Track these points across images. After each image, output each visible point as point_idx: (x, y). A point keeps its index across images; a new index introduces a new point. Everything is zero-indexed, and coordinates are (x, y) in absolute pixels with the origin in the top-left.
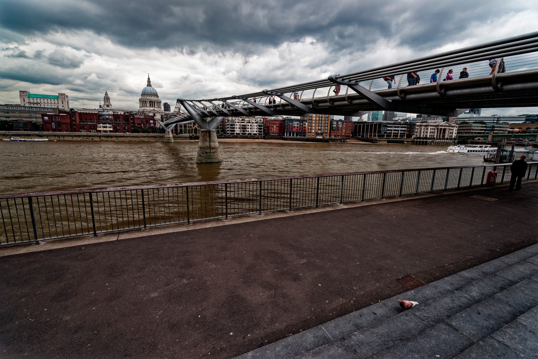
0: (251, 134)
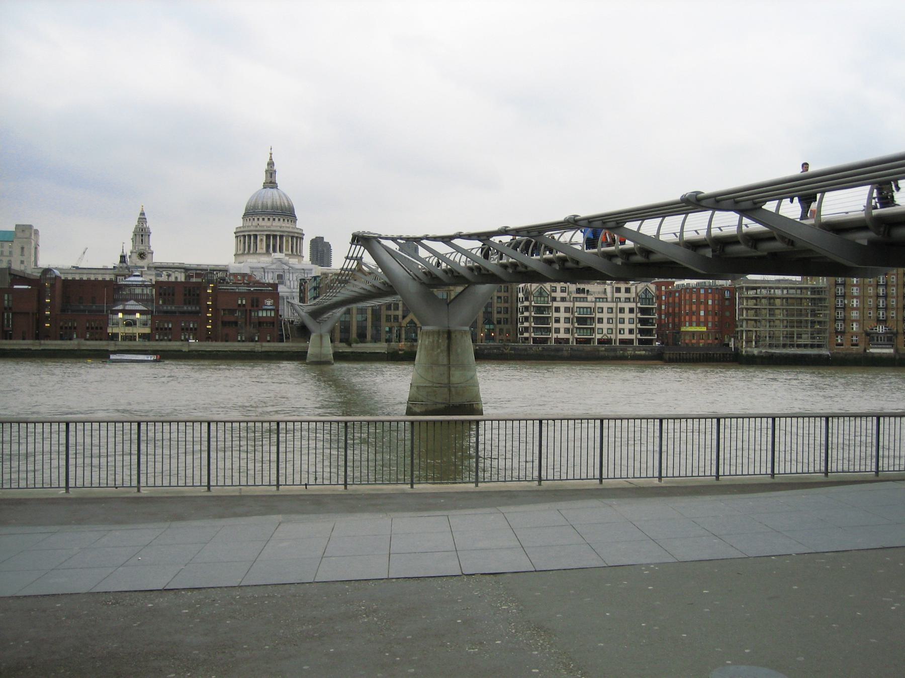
0: (609, 341)
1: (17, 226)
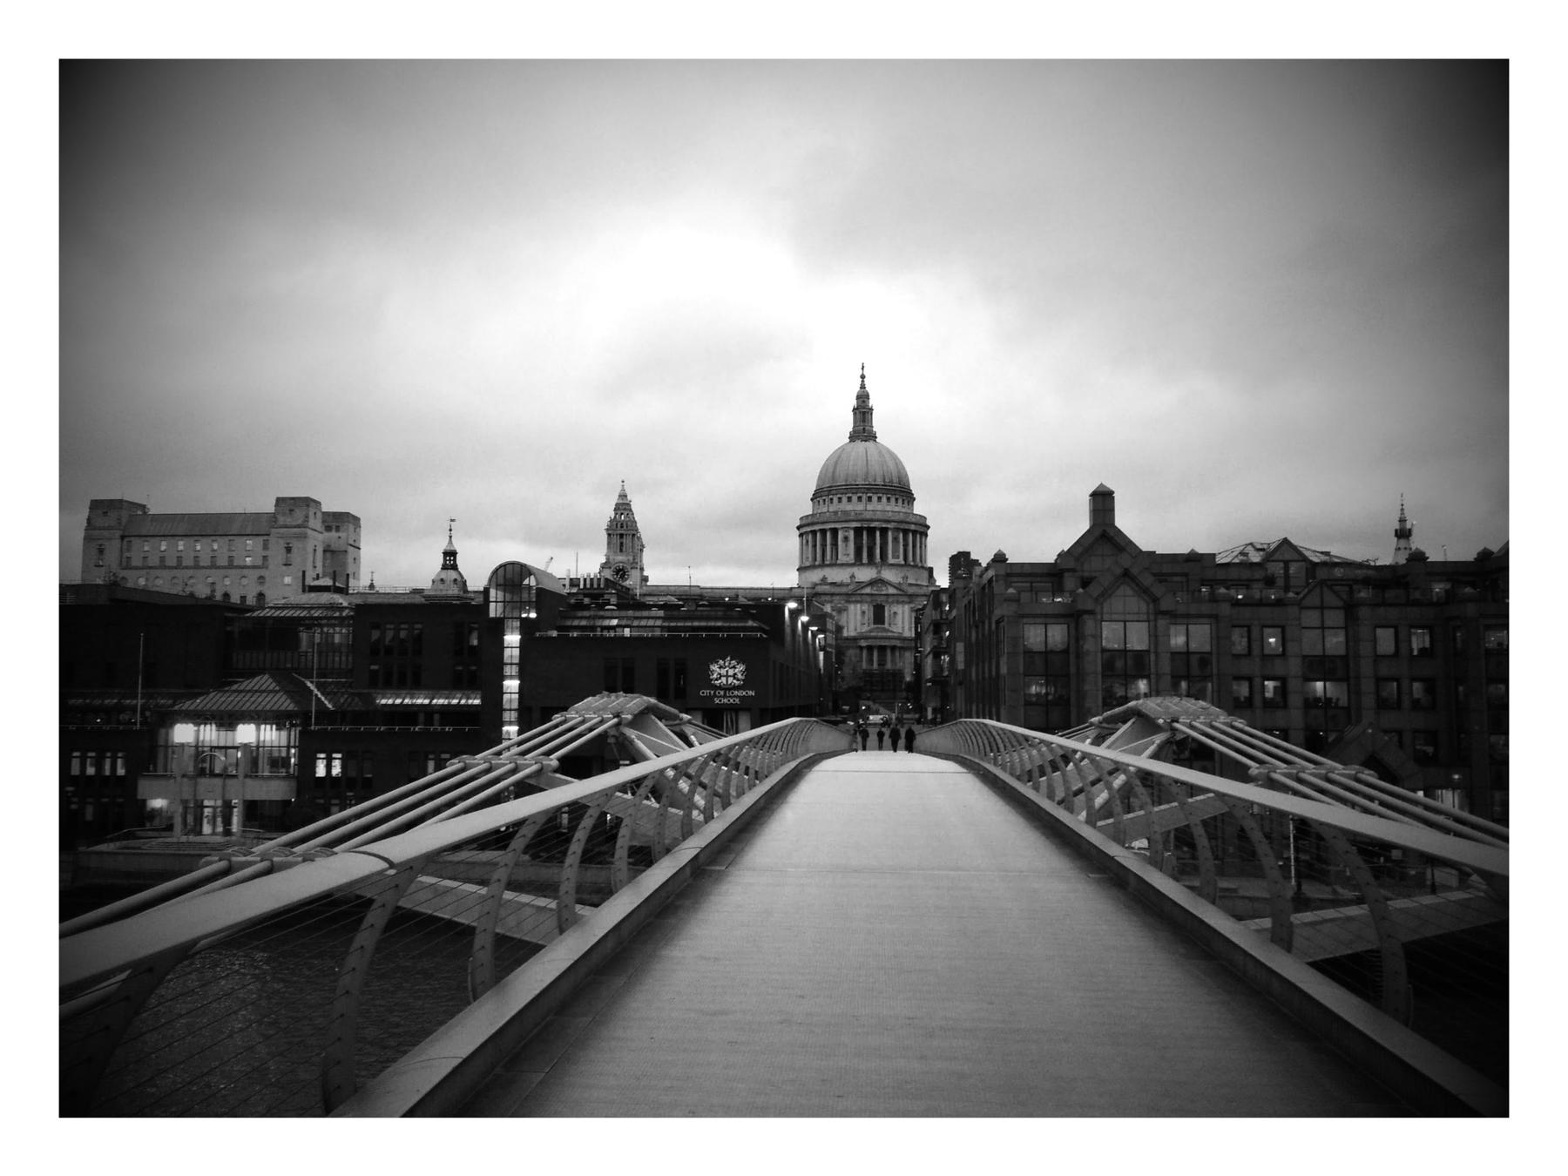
1: (279, 501)
